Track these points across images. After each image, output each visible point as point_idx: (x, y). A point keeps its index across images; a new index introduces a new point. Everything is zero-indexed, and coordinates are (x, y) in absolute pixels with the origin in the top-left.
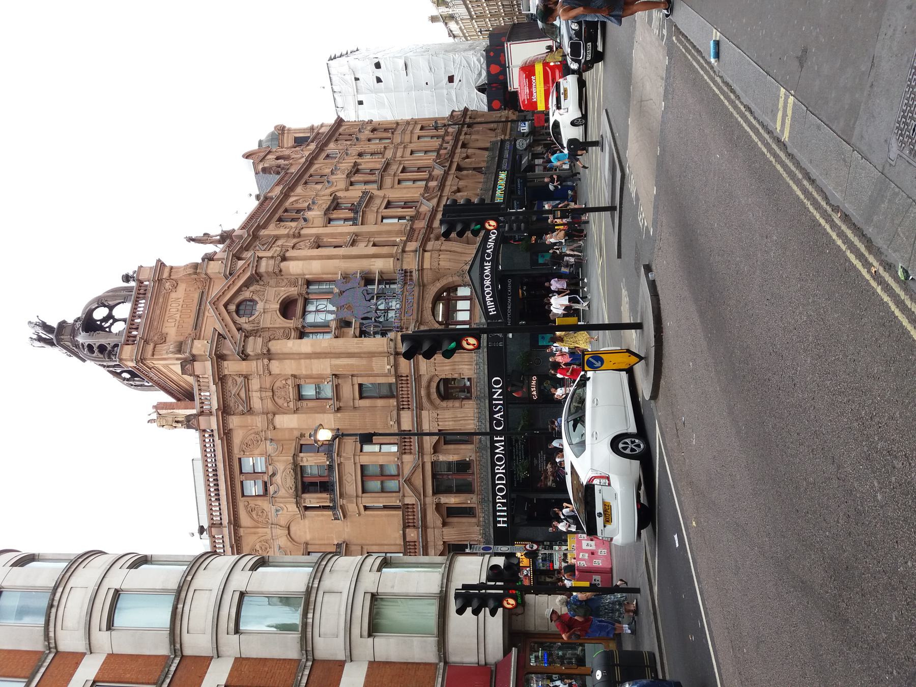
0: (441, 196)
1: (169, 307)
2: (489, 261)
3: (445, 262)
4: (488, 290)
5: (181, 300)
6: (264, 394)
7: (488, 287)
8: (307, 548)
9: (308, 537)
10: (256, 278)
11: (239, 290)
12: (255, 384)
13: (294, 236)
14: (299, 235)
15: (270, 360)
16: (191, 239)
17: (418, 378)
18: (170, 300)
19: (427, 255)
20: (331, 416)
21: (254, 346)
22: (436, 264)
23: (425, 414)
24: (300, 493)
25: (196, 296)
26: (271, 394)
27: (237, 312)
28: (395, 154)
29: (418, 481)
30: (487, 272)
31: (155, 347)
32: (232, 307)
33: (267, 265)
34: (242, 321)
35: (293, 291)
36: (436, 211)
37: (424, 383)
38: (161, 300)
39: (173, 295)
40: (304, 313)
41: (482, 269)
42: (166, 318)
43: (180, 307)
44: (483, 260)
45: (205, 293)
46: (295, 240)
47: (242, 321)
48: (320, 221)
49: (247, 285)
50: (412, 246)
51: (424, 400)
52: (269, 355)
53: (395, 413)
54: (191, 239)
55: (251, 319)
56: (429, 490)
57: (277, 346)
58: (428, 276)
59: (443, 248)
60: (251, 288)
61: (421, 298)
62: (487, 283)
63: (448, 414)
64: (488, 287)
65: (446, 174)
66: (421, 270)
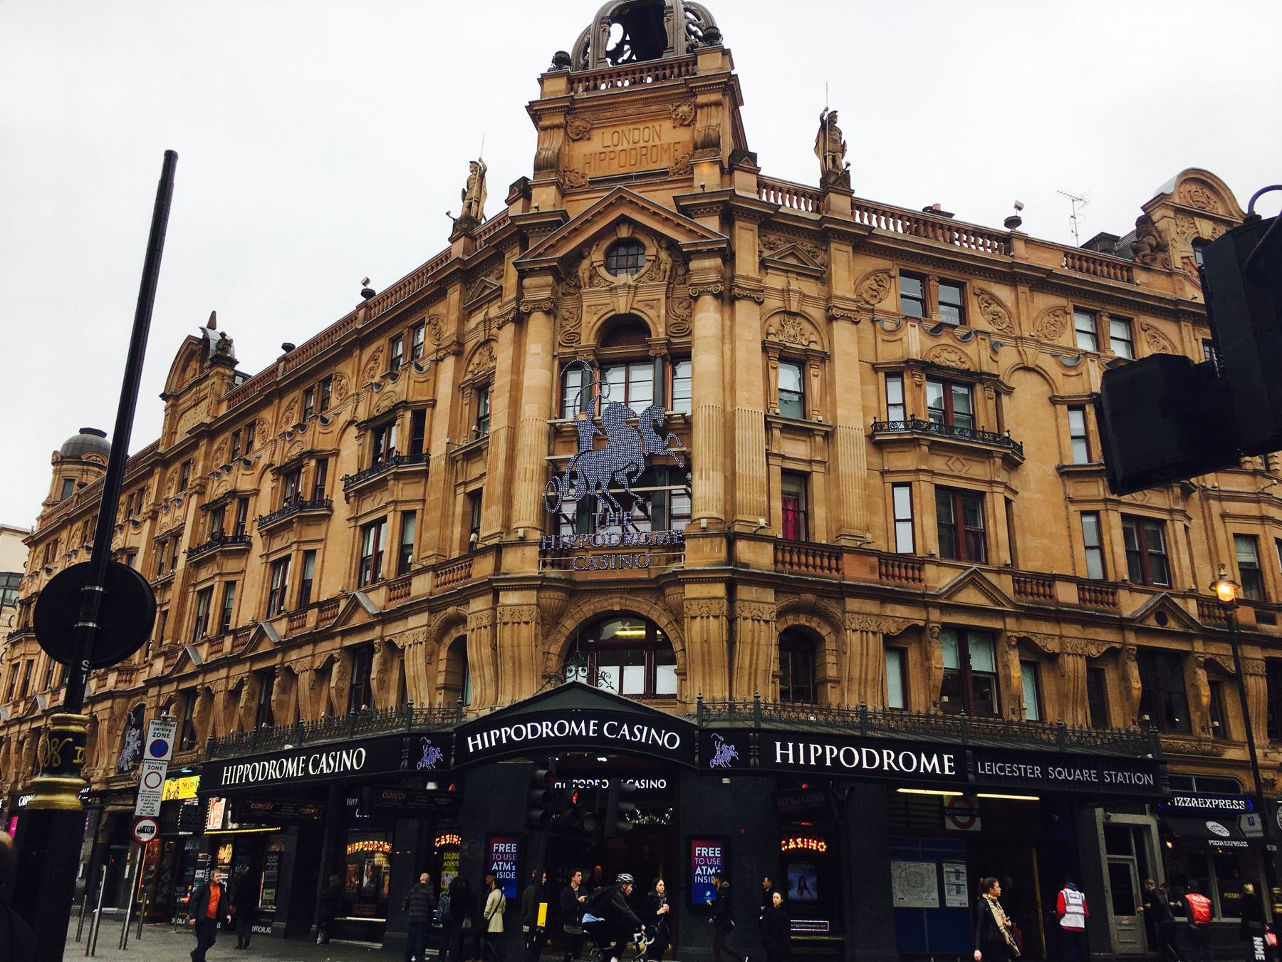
0: (1002, 615)
1: (642, 127)
2: (599, 730)
3: (703, 630)
4: (526, 730)
5: (657, 142)
6: (481, 327)
7: (534, 731)
8: (332, 455)
9: (343, 454)
10: (681, 257)
11: (659, 237)
12: (494, 311)
13: (828, 309)
14: (831, 319)
15: (513, 320)
16: (828, 125)
17: (464, 596)
18: (657, 124)
19: (719, 590)
20: (444, 451)
21: (539, 287)
22: (695, 610)
23: (423, 618)
24: (371, 425)
25: (664, 164)
26: (482, 340)
27: (620, 243)
28: (1235, 497)
29: (357, 620)
30: (572, 728)
31: (558, 127)
32: (624, 233)
33: (704, 271)
34: (597, 256)
35: (659, 331)
36: (926, 606)
37: (463, 610)
38: (654, 108)
39: (667, 125)
40: (627, 362)
41: (577, 717)
42: (619, 129)
43: (642, 144)
44: (602, 717)
45: (663, 178)
46: (816, 313)
47: (597, 256)
48: (891, 353)
49: (672, 245)
50: (758, 557)
51: (442, 615)
52: (520, 320)
53: (433, 561)
54: (828, 125)
55: (602, 271)
56: (350, 641)
57: (538, 326)
58: (672, 594)
59: (745, 627)
60: (663, 255)
61: (632, 587)
62: (545, 729)
63: (421, 660)
64: (534, 731)
65: (1123, 625)
66: (680, 579)
